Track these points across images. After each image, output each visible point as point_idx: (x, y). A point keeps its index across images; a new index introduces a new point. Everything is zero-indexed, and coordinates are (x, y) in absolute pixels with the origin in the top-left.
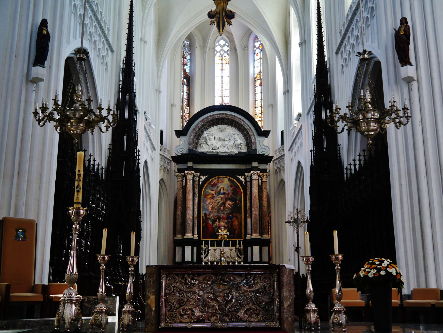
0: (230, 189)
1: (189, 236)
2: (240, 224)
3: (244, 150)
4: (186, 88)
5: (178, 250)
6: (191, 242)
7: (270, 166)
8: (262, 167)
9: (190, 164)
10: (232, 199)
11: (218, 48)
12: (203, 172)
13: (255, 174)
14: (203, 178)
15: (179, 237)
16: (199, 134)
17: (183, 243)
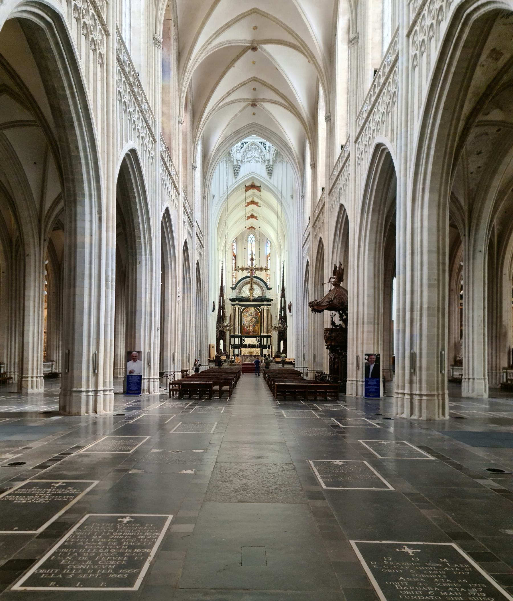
0: (254, 314)
1: (237, 333)
2: (259, 328)
3: (261, 296)
4: (234, 261)
5: (232, 339)
6: (237, 336)
7: (272, 302)
8: (269, 303)
9: (237, 302)
10: (256, 318)
11: (250, 239)
12: (243, 305)
13: (265, 307)
14: (243, 308)
15: (232, 334)
16: (241, 290)
17: (234, 336)
